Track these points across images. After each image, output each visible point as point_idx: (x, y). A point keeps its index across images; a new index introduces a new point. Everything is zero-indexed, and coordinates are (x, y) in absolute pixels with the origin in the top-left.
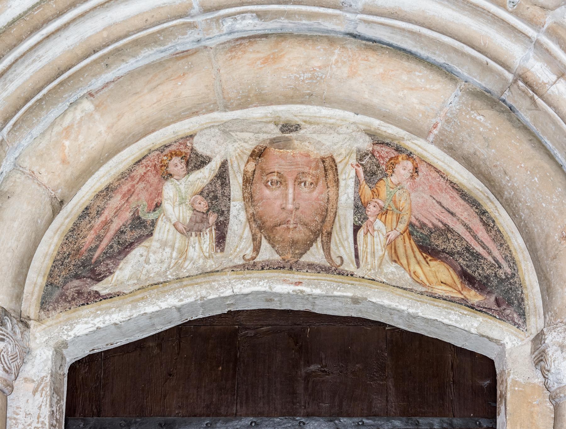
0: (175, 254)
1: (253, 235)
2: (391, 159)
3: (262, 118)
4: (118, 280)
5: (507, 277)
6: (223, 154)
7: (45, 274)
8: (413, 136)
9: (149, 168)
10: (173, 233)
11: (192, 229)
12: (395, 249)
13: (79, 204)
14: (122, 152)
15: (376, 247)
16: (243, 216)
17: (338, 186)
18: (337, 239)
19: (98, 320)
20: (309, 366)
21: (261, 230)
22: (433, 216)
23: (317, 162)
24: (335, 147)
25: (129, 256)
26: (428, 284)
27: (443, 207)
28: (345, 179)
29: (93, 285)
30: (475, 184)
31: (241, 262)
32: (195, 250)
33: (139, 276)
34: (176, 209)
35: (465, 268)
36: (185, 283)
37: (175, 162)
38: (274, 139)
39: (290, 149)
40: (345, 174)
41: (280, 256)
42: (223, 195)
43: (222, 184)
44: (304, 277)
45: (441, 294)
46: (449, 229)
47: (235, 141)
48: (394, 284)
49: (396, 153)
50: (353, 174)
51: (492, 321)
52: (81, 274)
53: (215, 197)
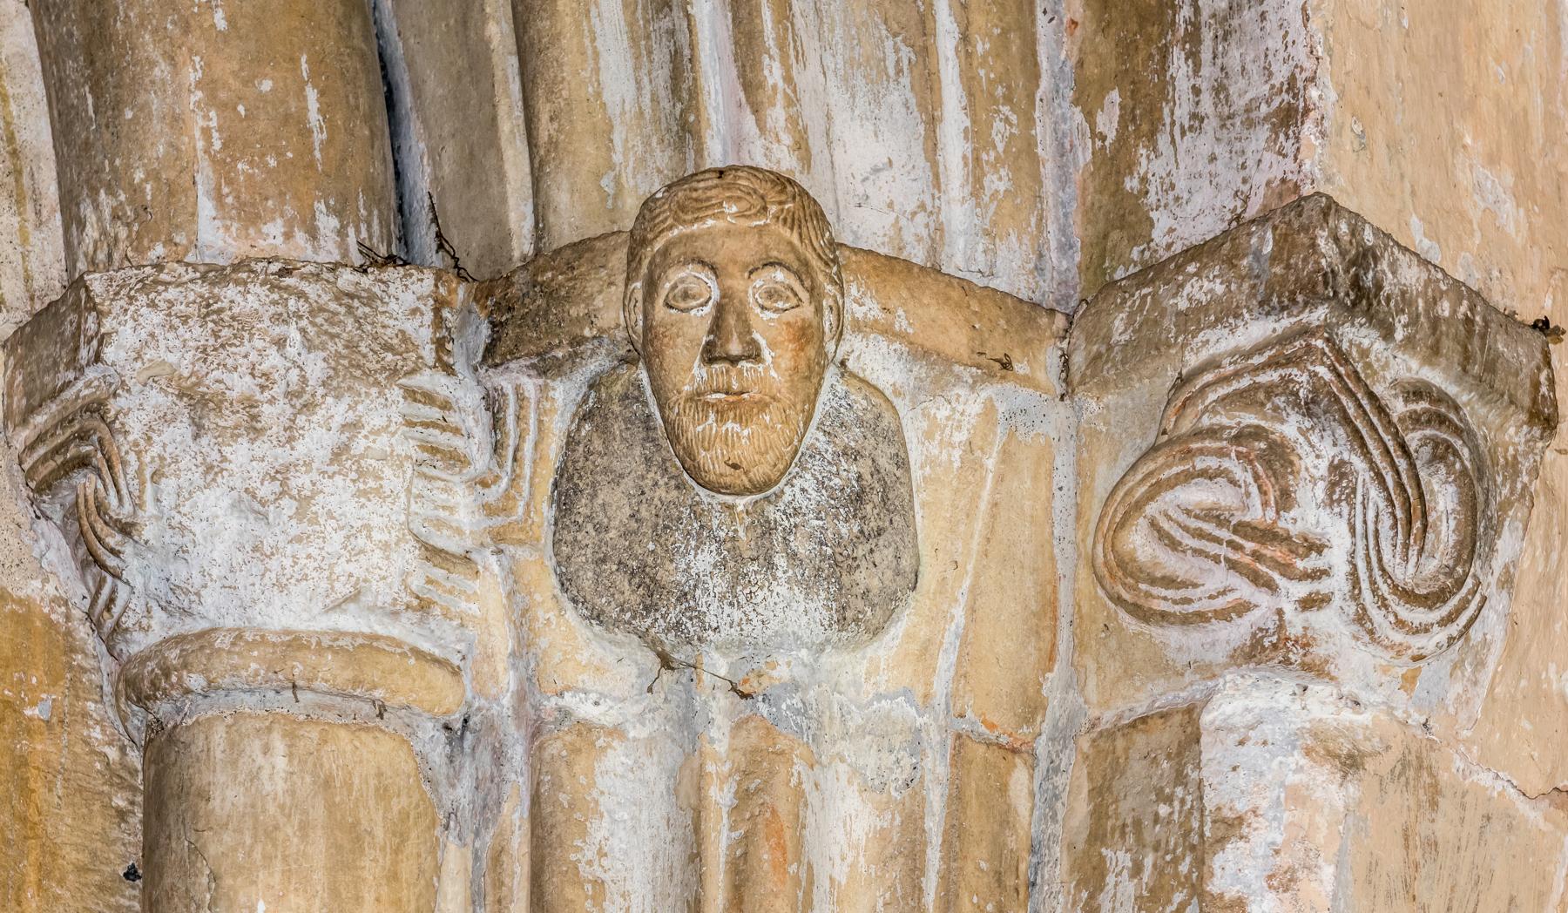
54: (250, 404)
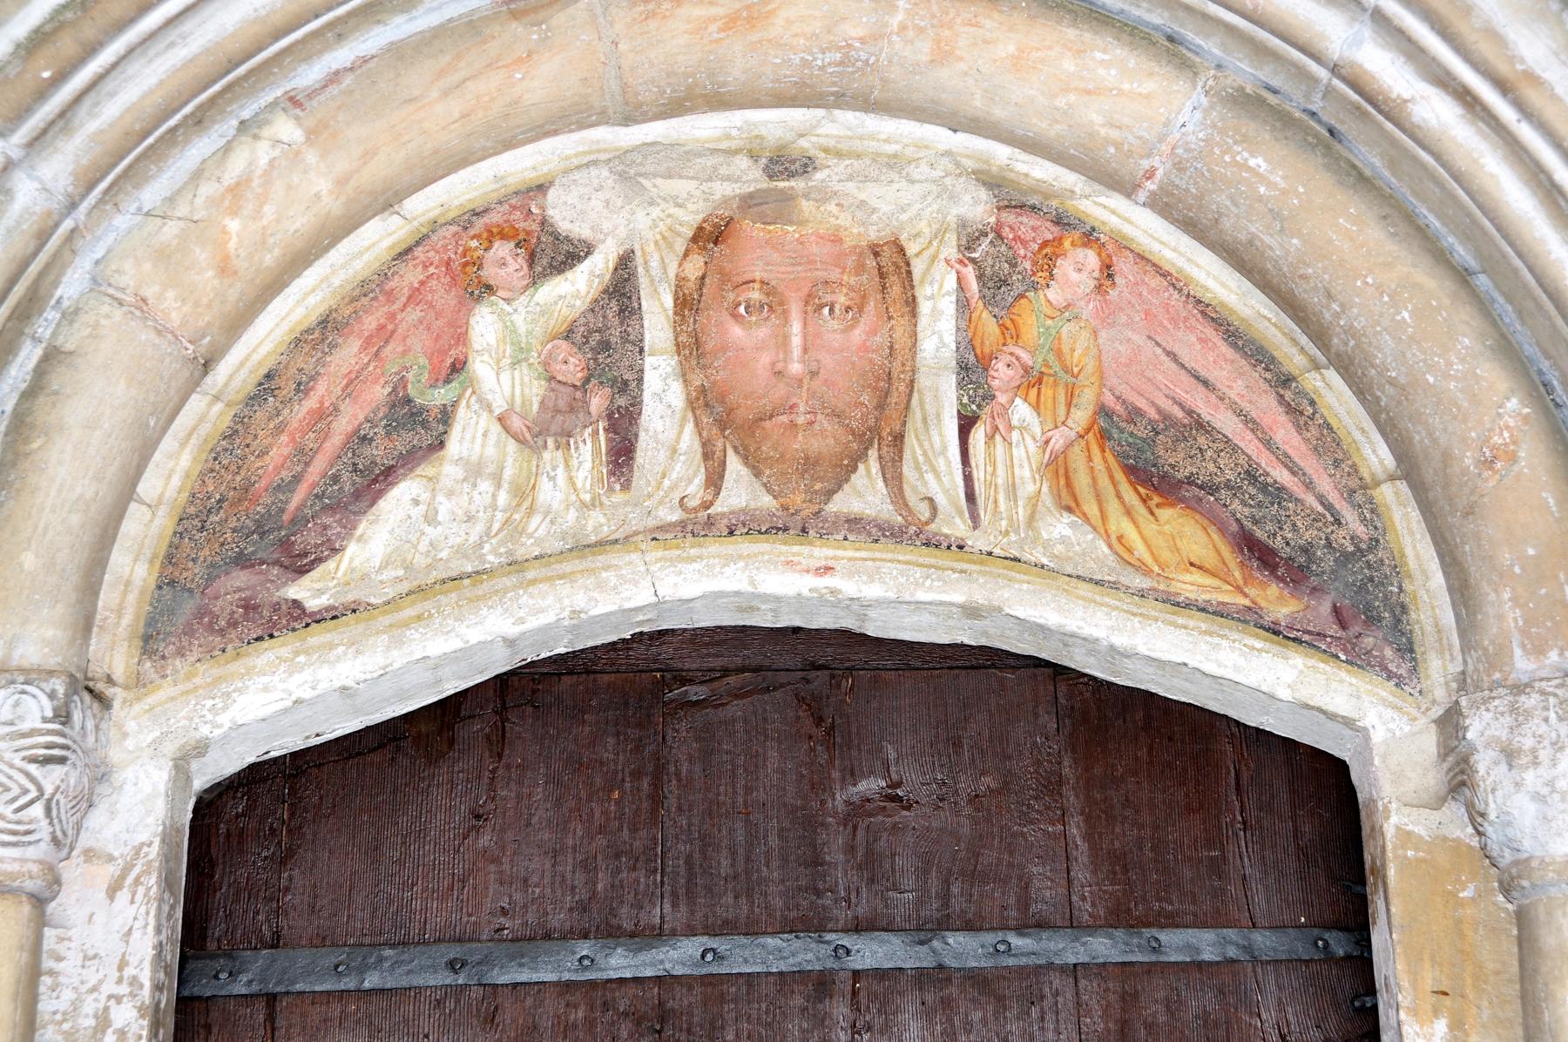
0: (503, 498)
1: (704, 445)
2: (1045, 244)
3: (719, 140)
4: (353, 570)
5: (1359, 549)
6: (623, 235)
7: (155, 556)
8: (1097, 187)
9: (432, 270)
10: (498, 442)
11: (543, 430)
12: (1067, 478)
13: (249, 365)
14: (363, 229)
15: (1017, 471)
16: (676, 395)
17: (914, 314)
18: (919, 452)
19: (297, 678)
20: (855, 785)
21: (723, 430)
22: (1158, 390)
23: (861, 254)
24: (904, 217)
25: (382, 503)
26: (1156, 569)
27: (1183, 366)
28: (932, 297)
29: (285, 584)
30: (1257, 306)
31: (675, 516)
32: (555, 485)
33: (410, 557)
34: (505, 377)
35: (1248, 524)
36: (530, 575)
37: (501, 253)
38: (751, 196)
39: (791, 223)
40: (931, 283)
41: (775, 497)
42: (625, 339)
43: (621, 311)
44: (840, 553)
45: (1192, 596)
46: (1201, 425)
47: (652, 203)
48: (1069, 570)
49: (1056, 230)
50: (951, 282)
51: (1328, 668)
52: (253, 553)
53: (604, 343)
54: (1534, 751)
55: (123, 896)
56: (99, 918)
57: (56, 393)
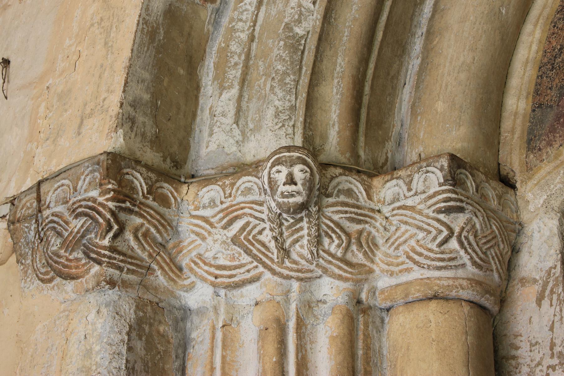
7: (528, 94)
55: (546, 303)
56: (535, 319)
57: (443, 10)
